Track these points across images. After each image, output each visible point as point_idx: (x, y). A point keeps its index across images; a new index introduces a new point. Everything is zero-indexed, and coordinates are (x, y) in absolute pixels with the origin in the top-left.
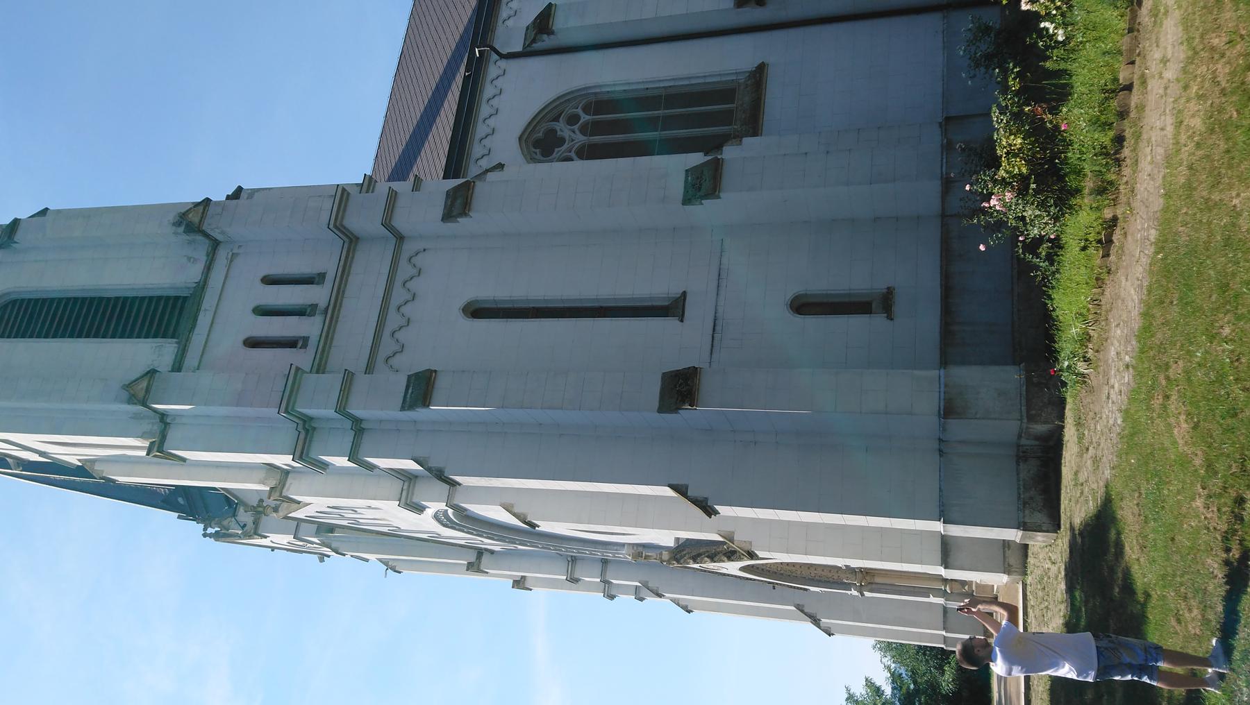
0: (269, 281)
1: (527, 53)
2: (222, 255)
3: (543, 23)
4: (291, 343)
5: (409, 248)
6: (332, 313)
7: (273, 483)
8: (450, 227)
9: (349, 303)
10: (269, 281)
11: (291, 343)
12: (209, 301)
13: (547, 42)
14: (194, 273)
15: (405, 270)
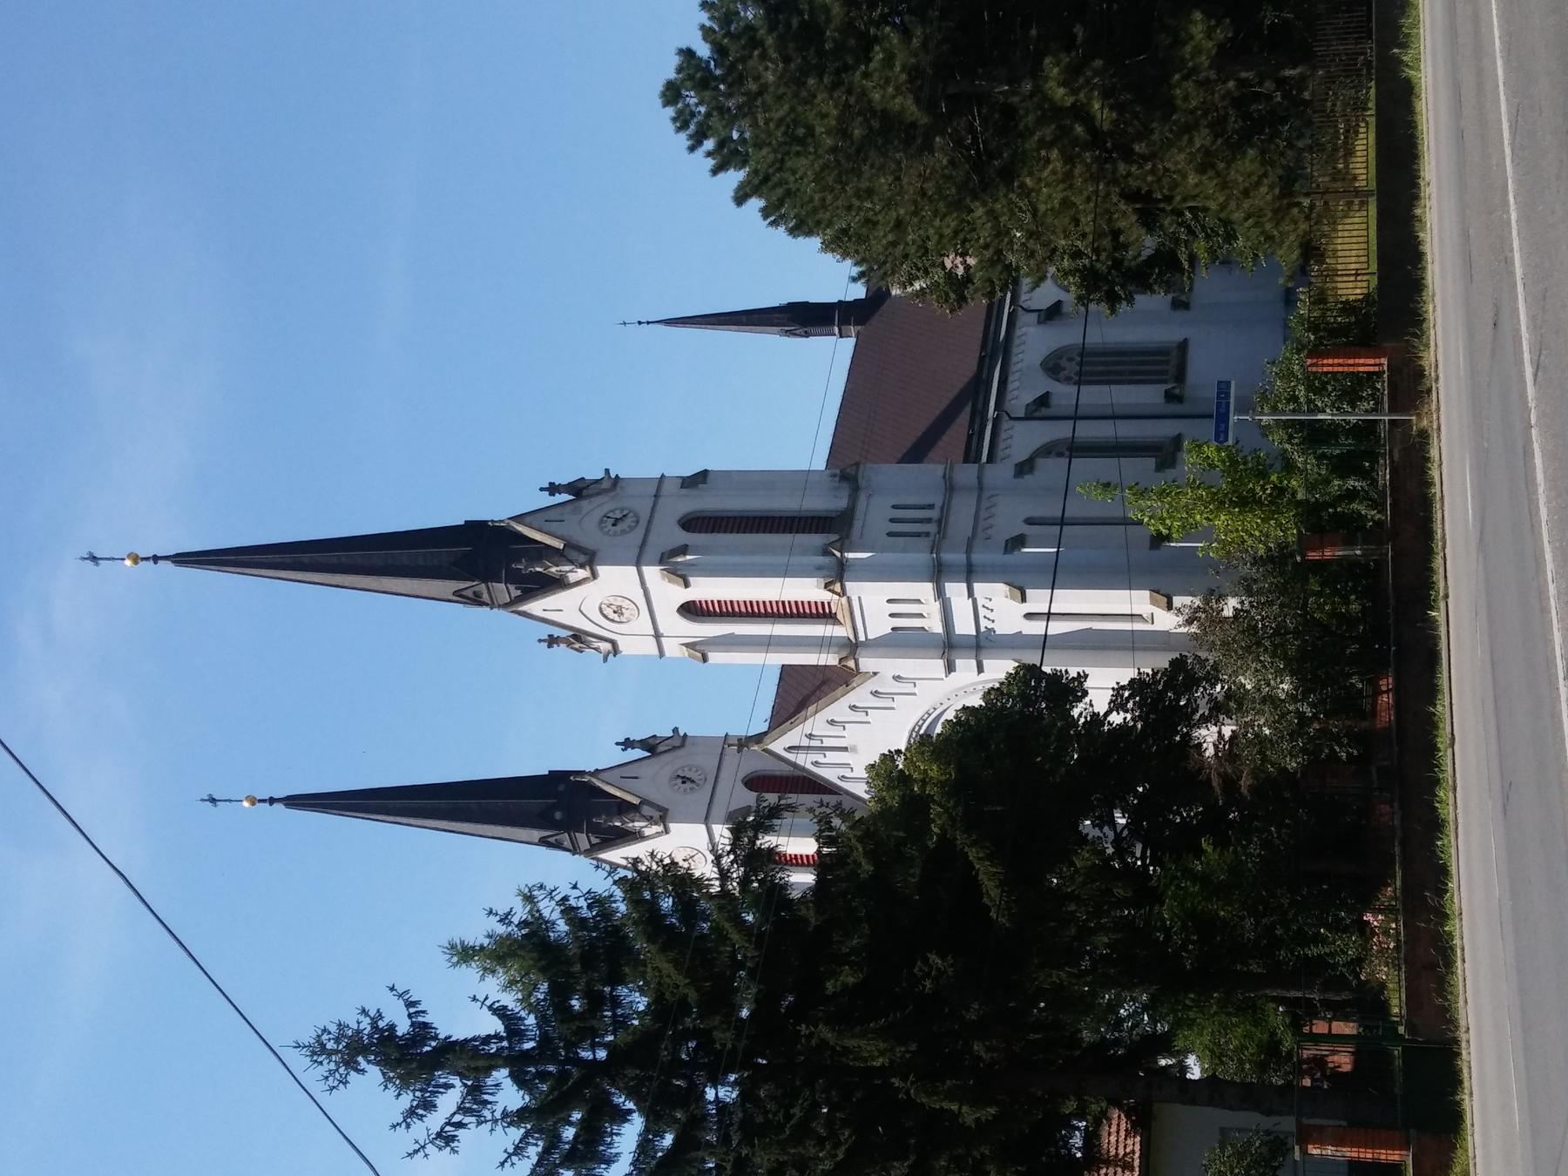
0: (895, 507)
1: (1029, 417)
2: (862, 497)
3: (1043, 401)
4: (918, 535)
5: (986, 494)
6: (942, 523)
7: (844, 654)
8: (1019, 480)
9: (952, 519)
10: (895, 507)
11: (918, 535)
12: (859, 514)
13: (1044, 412)
14: (842, 503)
15: (985, 504)
